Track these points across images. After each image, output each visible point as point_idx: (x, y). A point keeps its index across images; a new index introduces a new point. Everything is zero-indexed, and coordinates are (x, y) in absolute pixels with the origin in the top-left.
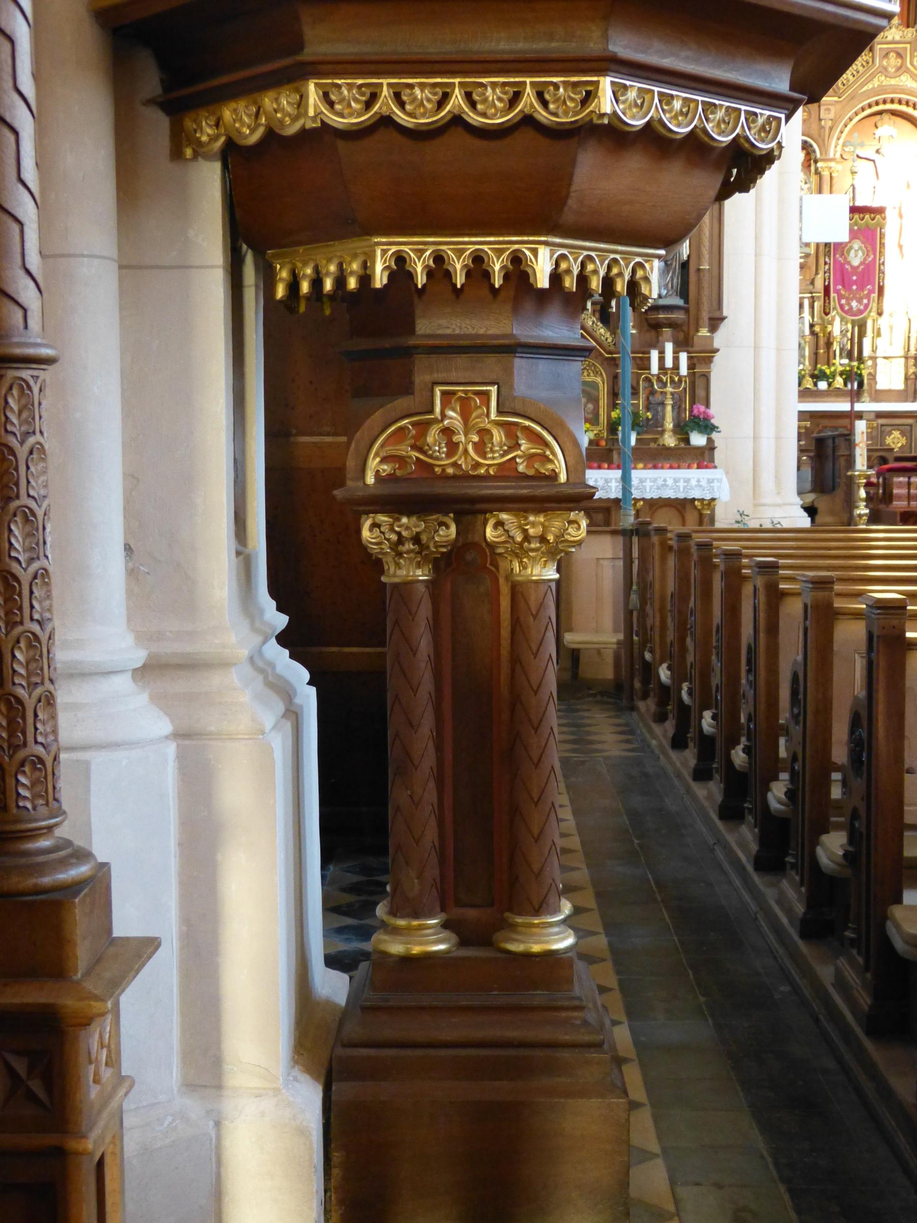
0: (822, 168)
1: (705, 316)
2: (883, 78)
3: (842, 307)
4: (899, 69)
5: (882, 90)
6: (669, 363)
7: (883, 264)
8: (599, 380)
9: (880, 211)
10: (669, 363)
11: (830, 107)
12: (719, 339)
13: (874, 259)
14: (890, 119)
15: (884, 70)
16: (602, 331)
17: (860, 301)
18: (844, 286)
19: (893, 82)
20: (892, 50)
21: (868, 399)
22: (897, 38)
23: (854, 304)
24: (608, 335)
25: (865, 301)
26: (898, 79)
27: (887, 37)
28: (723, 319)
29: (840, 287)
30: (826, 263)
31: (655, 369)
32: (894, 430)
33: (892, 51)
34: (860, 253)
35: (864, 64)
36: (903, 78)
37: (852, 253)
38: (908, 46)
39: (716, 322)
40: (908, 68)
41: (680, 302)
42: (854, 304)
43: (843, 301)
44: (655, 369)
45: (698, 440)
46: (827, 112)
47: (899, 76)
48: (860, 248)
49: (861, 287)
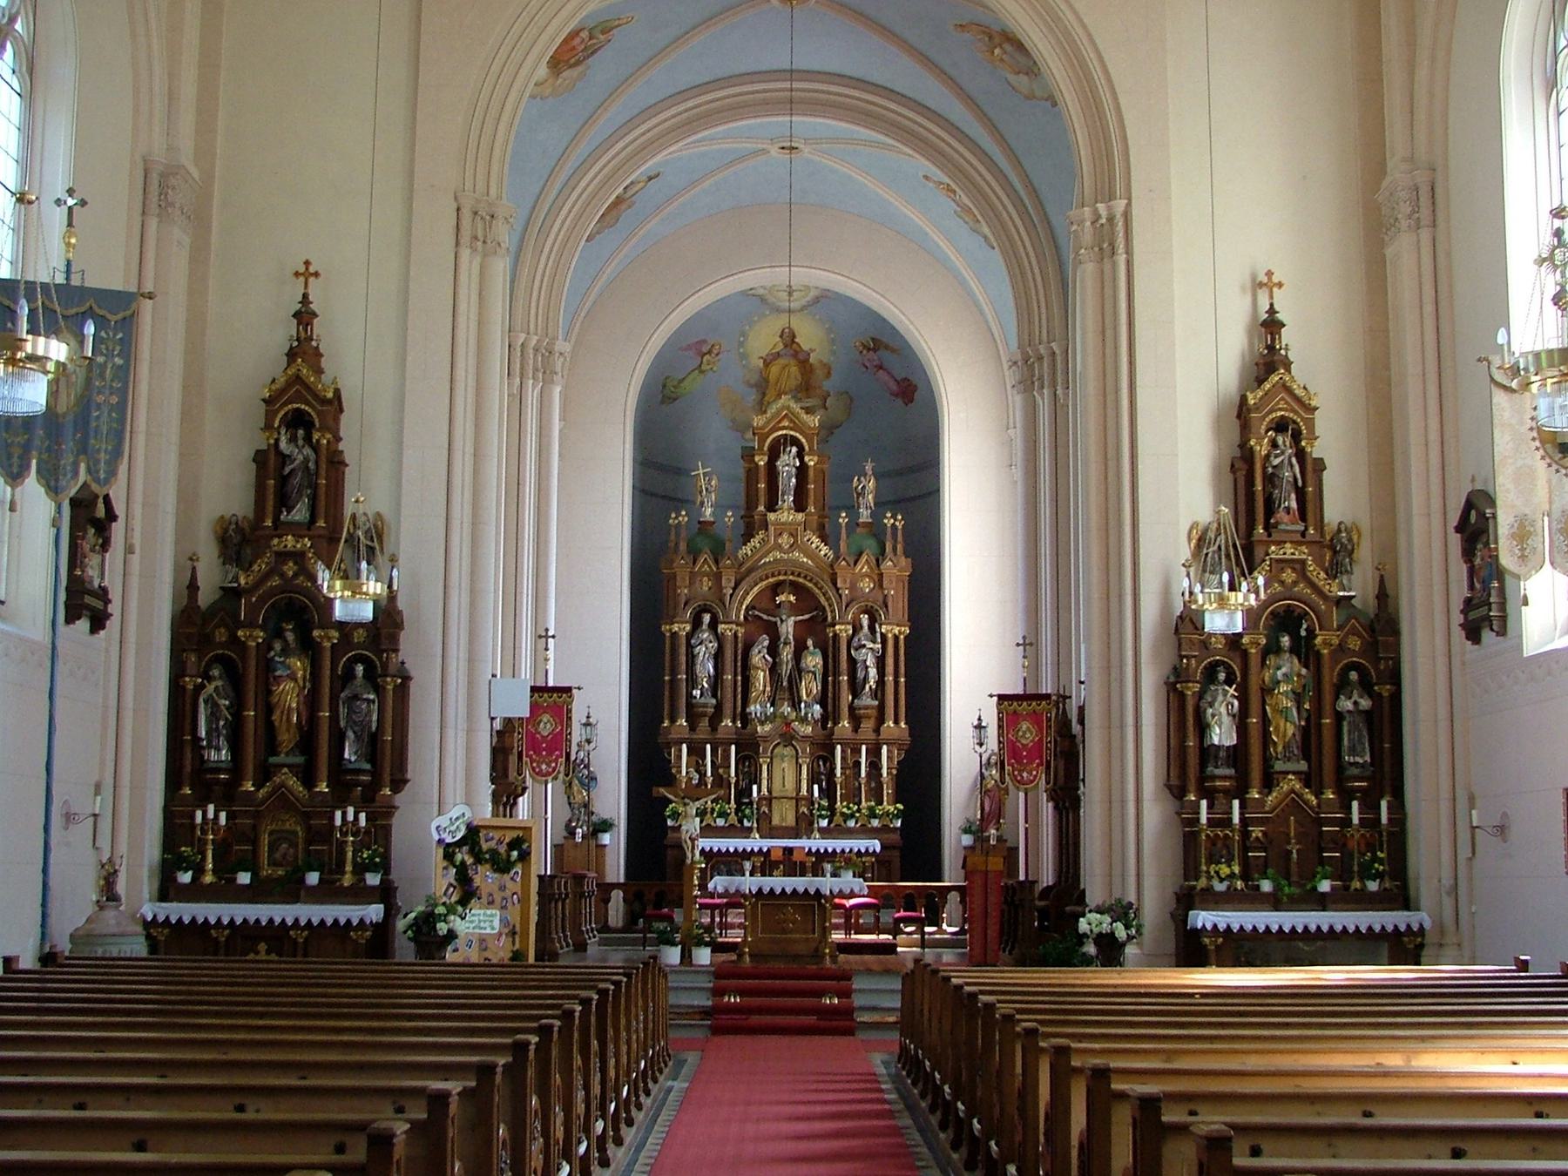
1: (387, 778)
3: (533, 769)
4: (791, 546)
6: (350, 817)
7: (570, 734)
8: (299, 829)
9: (568, 690)
10: (350, 817)
12: (399, 799)
13: (562, 729)
15: (779, 547)
16: (301, 789)
17: (548, 765)
18: (535, 753)
19: (786, 557)
21: (757, 836)
23: (544, 767)
24: (305, 792)
25: (553, 765)
28: (406, 781)
29: (532, 753)
30: (519, 733)
31: (338, 822)
34: (548, 726)
37: (542, 725)
39: (399, 783)
40: (799, 546)
41: (368, 767)
42: (544, 767)
43: (535, 765)
44: (338, 822)
45: (373, 879)
48: (549, 721)
49: (550, 753)
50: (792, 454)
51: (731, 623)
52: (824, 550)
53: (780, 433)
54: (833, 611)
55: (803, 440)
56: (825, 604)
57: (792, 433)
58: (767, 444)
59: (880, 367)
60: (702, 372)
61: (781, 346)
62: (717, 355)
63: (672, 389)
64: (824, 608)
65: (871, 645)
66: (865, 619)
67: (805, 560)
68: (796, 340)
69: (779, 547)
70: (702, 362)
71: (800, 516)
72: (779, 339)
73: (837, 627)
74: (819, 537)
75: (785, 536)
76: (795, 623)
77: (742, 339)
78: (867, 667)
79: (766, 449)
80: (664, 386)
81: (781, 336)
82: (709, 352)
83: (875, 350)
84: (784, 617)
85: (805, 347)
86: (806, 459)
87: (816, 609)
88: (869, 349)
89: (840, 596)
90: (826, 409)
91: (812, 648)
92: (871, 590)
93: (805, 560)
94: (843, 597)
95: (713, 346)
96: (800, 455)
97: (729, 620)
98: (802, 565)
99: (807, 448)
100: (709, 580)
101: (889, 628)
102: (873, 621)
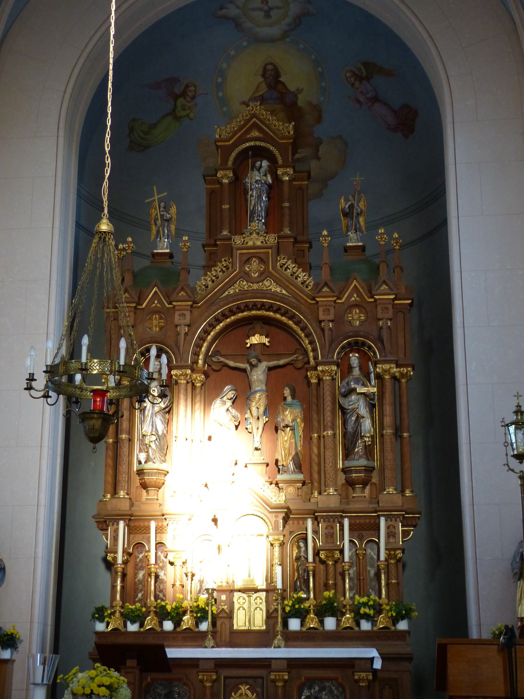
0: (176, 375)
2: (245, 283)
4: (261, 274)
5: (243, 293)
11: (185, 312)
14: (262, 328)
15: (246, 276)
19: (255, 286)
20: (254, 256)
21: (212, 643)
22: (258, 243)
26: (261, 284)
27: (247, 243)
32: (242, 684)
33: (255, 257)
35: (224, 269)
36: (267, 283)
38: (270, 251)
46: (182, 317)
47: (262, 281)
50: (262, 170)
51: (185, 367)
52: (302, 276)
53: (248, 144)
54: (314, 350)
55: (276, 153)
56: (309, 348)
57: (262, 144)
58: (231, 158)
59: (375, 99)
60: (177, 118)
61: (264, 88)
62: (193, 98)
63: (141, 134)
64: (305, 353)
65: (364, 390)
66: (354, 359)
67: (278, 290)
68: (281, 79)
69: (246, 276)
70: (175, 106)
71: (272, 239)
72: (261, 79)
73: (320, 368)
74: (295, 262)
75: (255, 263)
76: (270, 369)
77: (220, 80)
78: (359, 417)
79: (230, 163)
80: (131, 130)
81: (264, 75)
82: (184, 94)
83: (368, 78)
84: (254, 361)
85: (292, 87)
86: (280, 172)
87: (294, 354)
88: (360, 79)
89: (323, 330)
90: (319, 159)
91: (289, 399)
92: (362, 323)
93: (278, 290)
94: (327, 332)
95: (187, 86)
96: (272, 171)
97: (183, 364)
98: (274, 296)
99: (280, 161)
100: (161, 318)
101: (386, 366)
102: (365, 359)
